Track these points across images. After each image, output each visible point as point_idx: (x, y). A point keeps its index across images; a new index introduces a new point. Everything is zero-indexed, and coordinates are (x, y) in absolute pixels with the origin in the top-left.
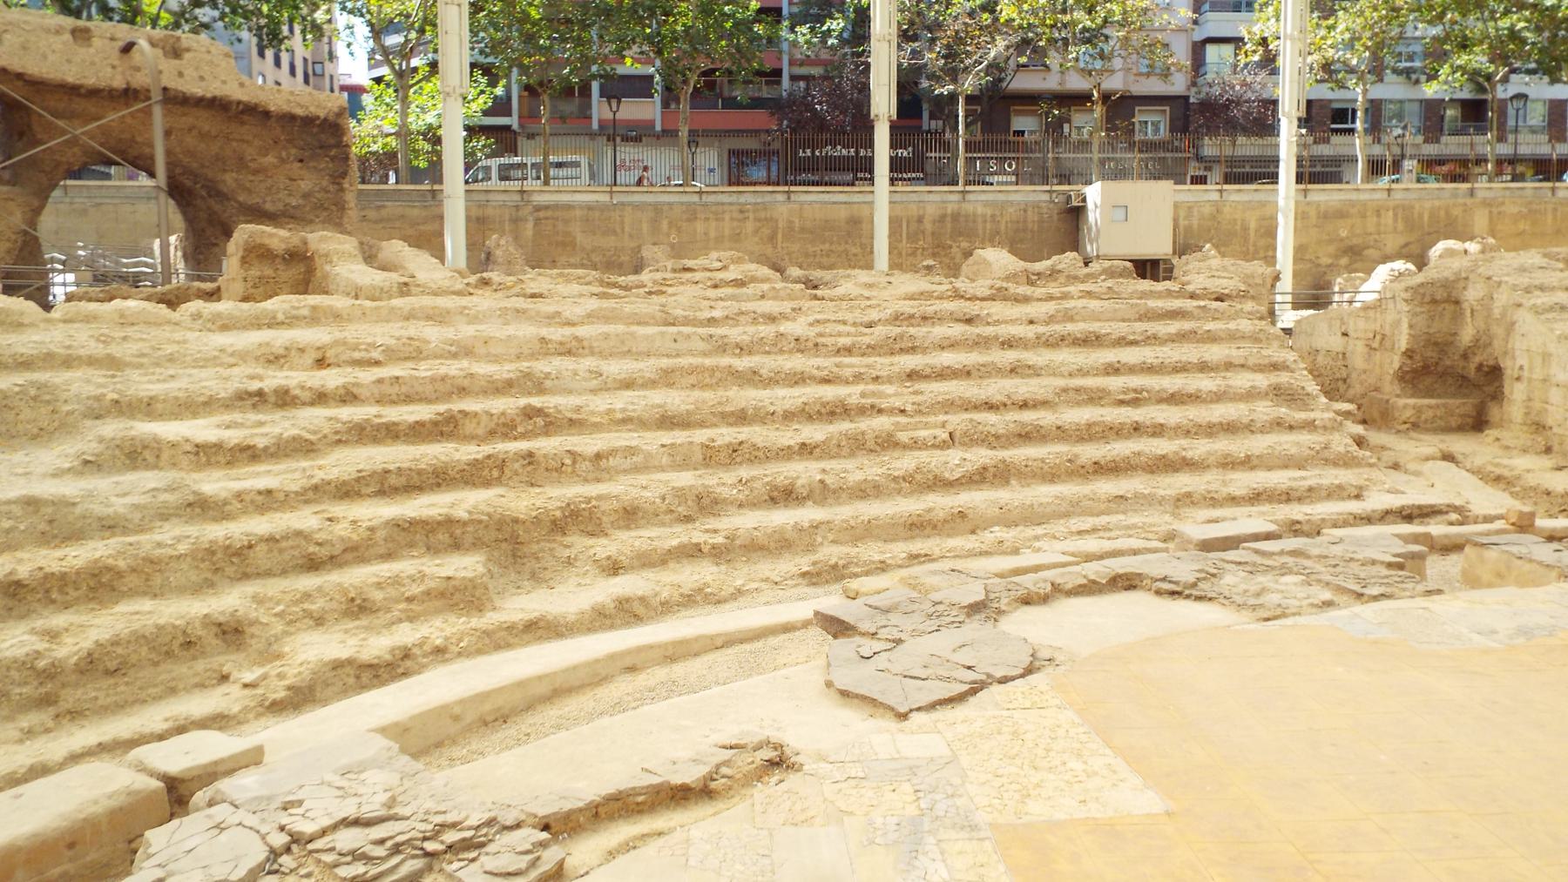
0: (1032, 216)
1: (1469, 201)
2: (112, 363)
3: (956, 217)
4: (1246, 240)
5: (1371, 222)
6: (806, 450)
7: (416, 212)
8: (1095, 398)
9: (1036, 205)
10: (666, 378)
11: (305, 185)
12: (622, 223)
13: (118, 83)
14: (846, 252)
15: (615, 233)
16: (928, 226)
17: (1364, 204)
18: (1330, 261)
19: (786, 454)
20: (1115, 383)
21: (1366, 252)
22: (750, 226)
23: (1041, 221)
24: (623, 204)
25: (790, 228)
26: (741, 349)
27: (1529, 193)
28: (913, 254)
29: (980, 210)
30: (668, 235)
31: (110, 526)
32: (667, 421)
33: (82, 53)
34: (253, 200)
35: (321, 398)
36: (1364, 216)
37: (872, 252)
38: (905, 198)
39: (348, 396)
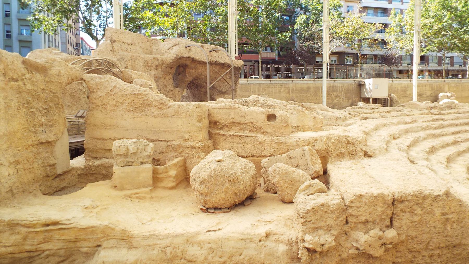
0: (350, 87)
1: (444, 83)
3: (333, 87)
4: (398, 92)
5: (424, 88)
9: (351, 84)
12: (250, 89)
15: (249, 91)
17: (423, 84)
22: (283, 89)
23: (352, 88)
24: (251, 83)
25: (293, 90)
27: (456, 81)
30: (262, 92)
37: (322, 97)
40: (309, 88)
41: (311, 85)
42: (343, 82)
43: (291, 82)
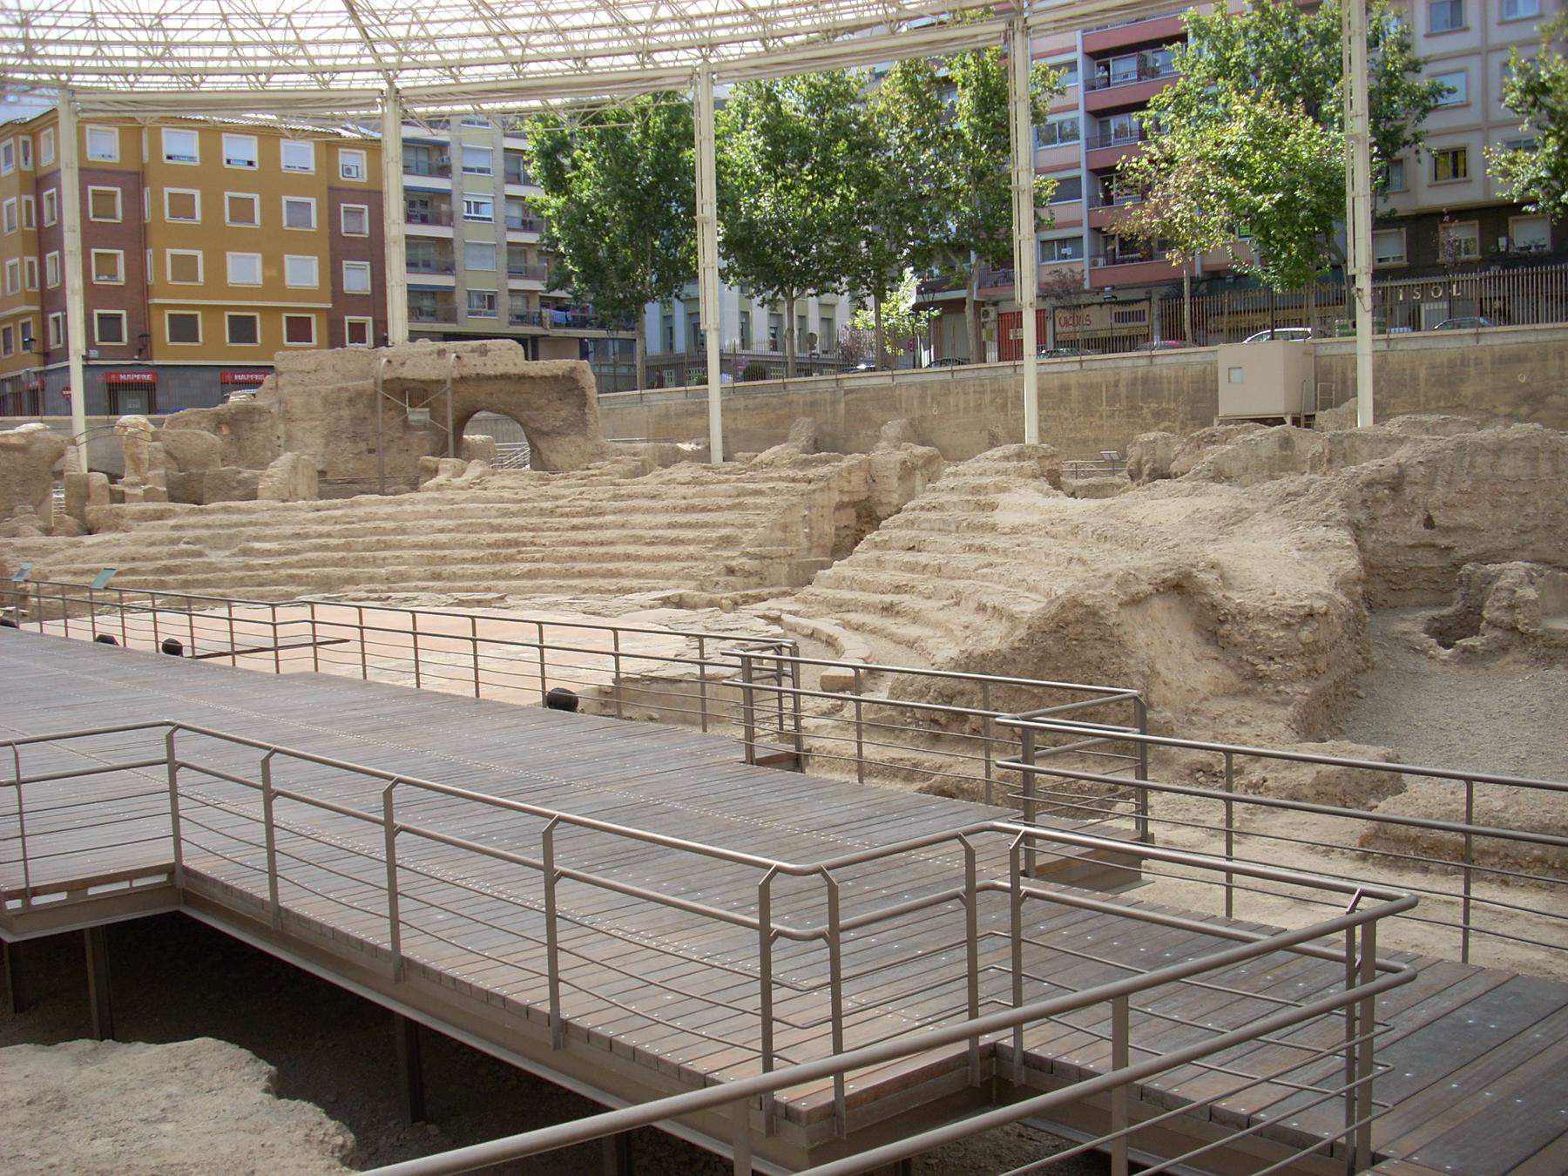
2: (267, 524)
3: (1145, 380)
6: (474, 560)
7: (775, 401)
8: (637, 540)
10: (458, 529)
11: (563, 414)
13: (456, 375)
14: (1059, 416)
16: (1123, 390)
18: (1509, 410)
19: (464, 561)
20: (672, 533)
21: (1549, 399)
22: (988, 398)
26: (514, 514)
28: (1112, 416)
29: (1165, 372)
31: (221, 570)
32: (434, 546)
33: (441, 362)
34: (537, 425)
35: (320, 536)
36: (1546, 359)
38: (1103, 365)
39: (329, 535)
40: (1065, 388)
41: (1073, 380)
42: (1183, 359)
43: (1010, 371)
